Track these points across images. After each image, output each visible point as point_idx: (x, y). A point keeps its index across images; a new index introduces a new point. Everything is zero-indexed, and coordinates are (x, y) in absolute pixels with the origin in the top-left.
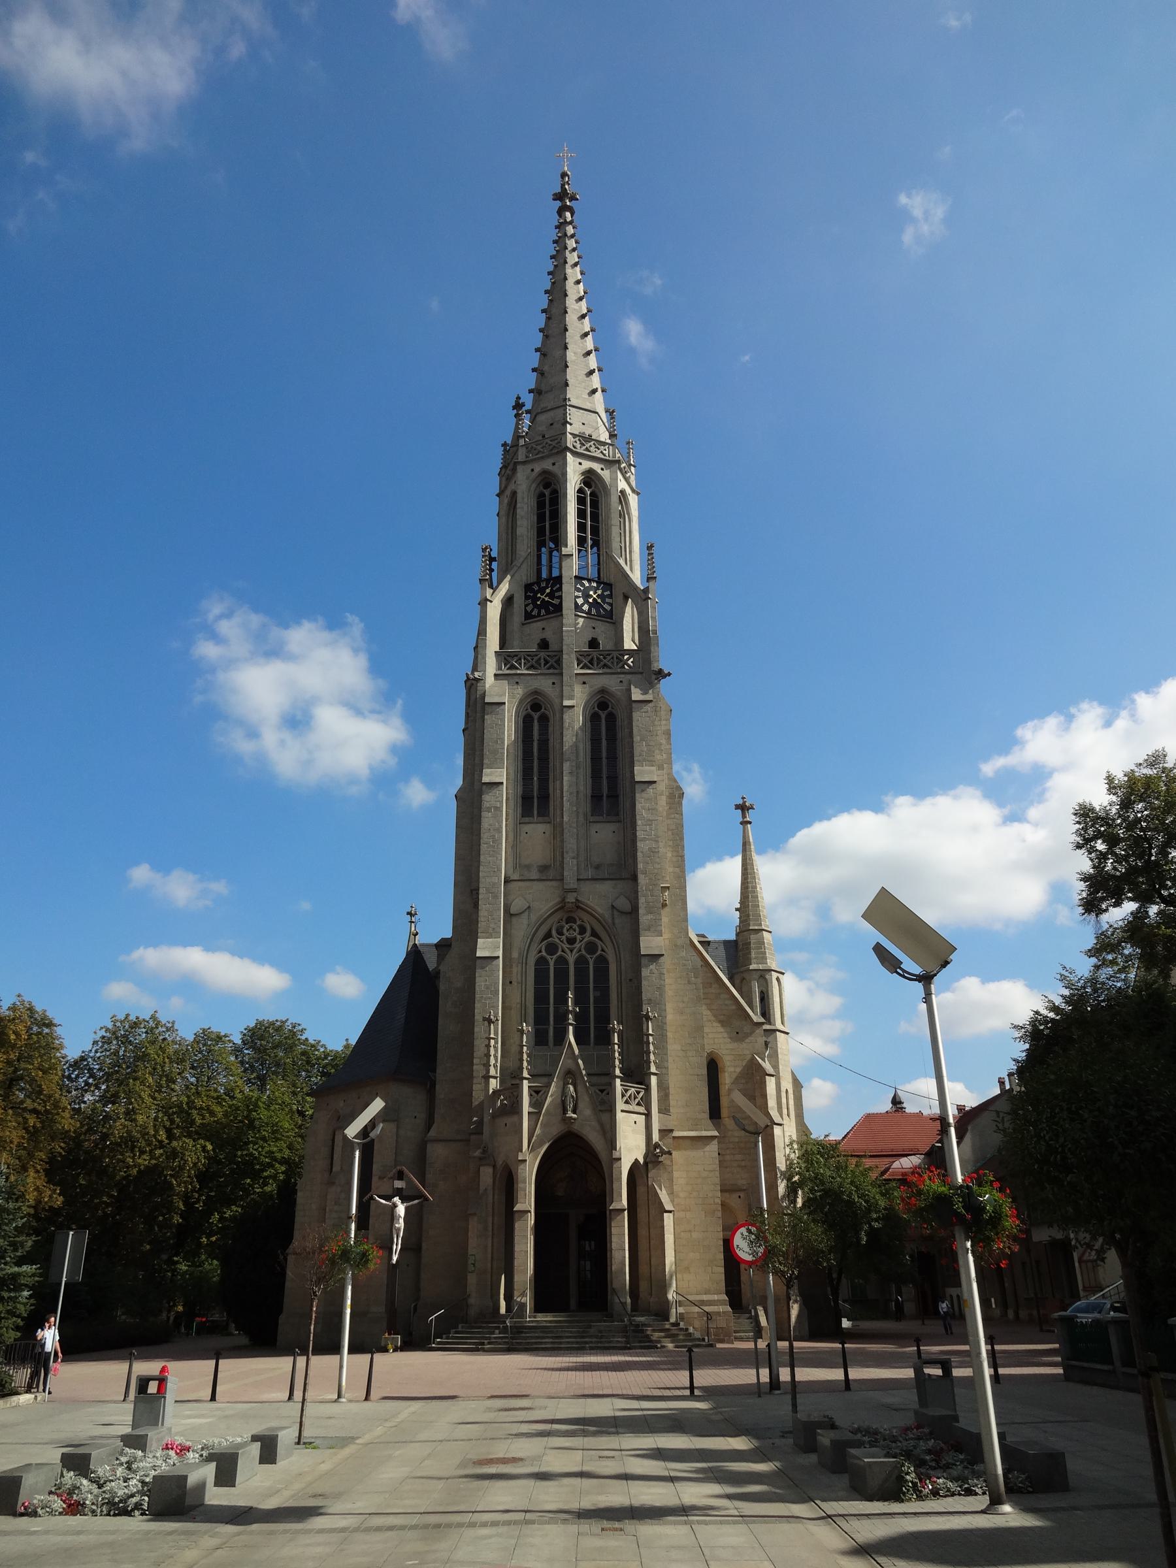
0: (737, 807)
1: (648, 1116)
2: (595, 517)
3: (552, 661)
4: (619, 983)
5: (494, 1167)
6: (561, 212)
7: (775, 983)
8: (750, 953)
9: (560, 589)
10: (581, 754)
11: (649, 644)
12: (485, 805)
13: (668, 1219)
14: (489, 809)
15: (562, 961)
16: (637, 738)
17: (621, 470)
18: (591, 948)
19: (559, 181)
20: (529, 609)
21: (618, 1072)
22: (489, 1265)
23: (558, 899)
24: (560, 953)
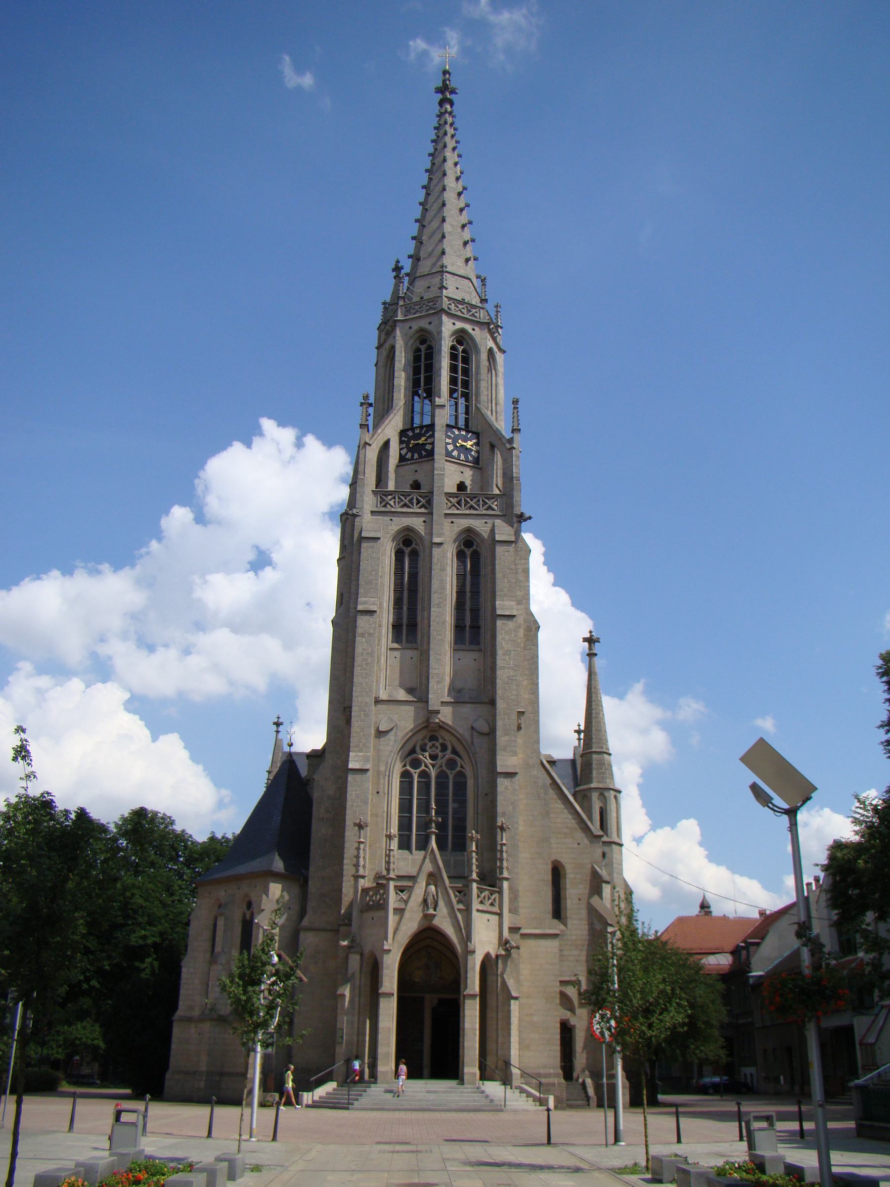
0: (585, 640)
1: (500, 915)
2: (466, 372)
3: (423, 501)
4: (477, 797)
5: (362, 954)
6: (441, 103)
7: (613, 800)
8: (591, 773)
9: (433, 436)
10: (448, 587)
11: (512, 489)
12: (359, 631)
13: (514, 1006)
14: (363, 635)
15: (424, 775)
16: (499, 575)
17: (490, 331)
18: (451, 764)
19: (441, 78)
20: (404, 452)
21: (474, 876)
22: (355, 1038)
23: (423, 719)
24: (423, 767)
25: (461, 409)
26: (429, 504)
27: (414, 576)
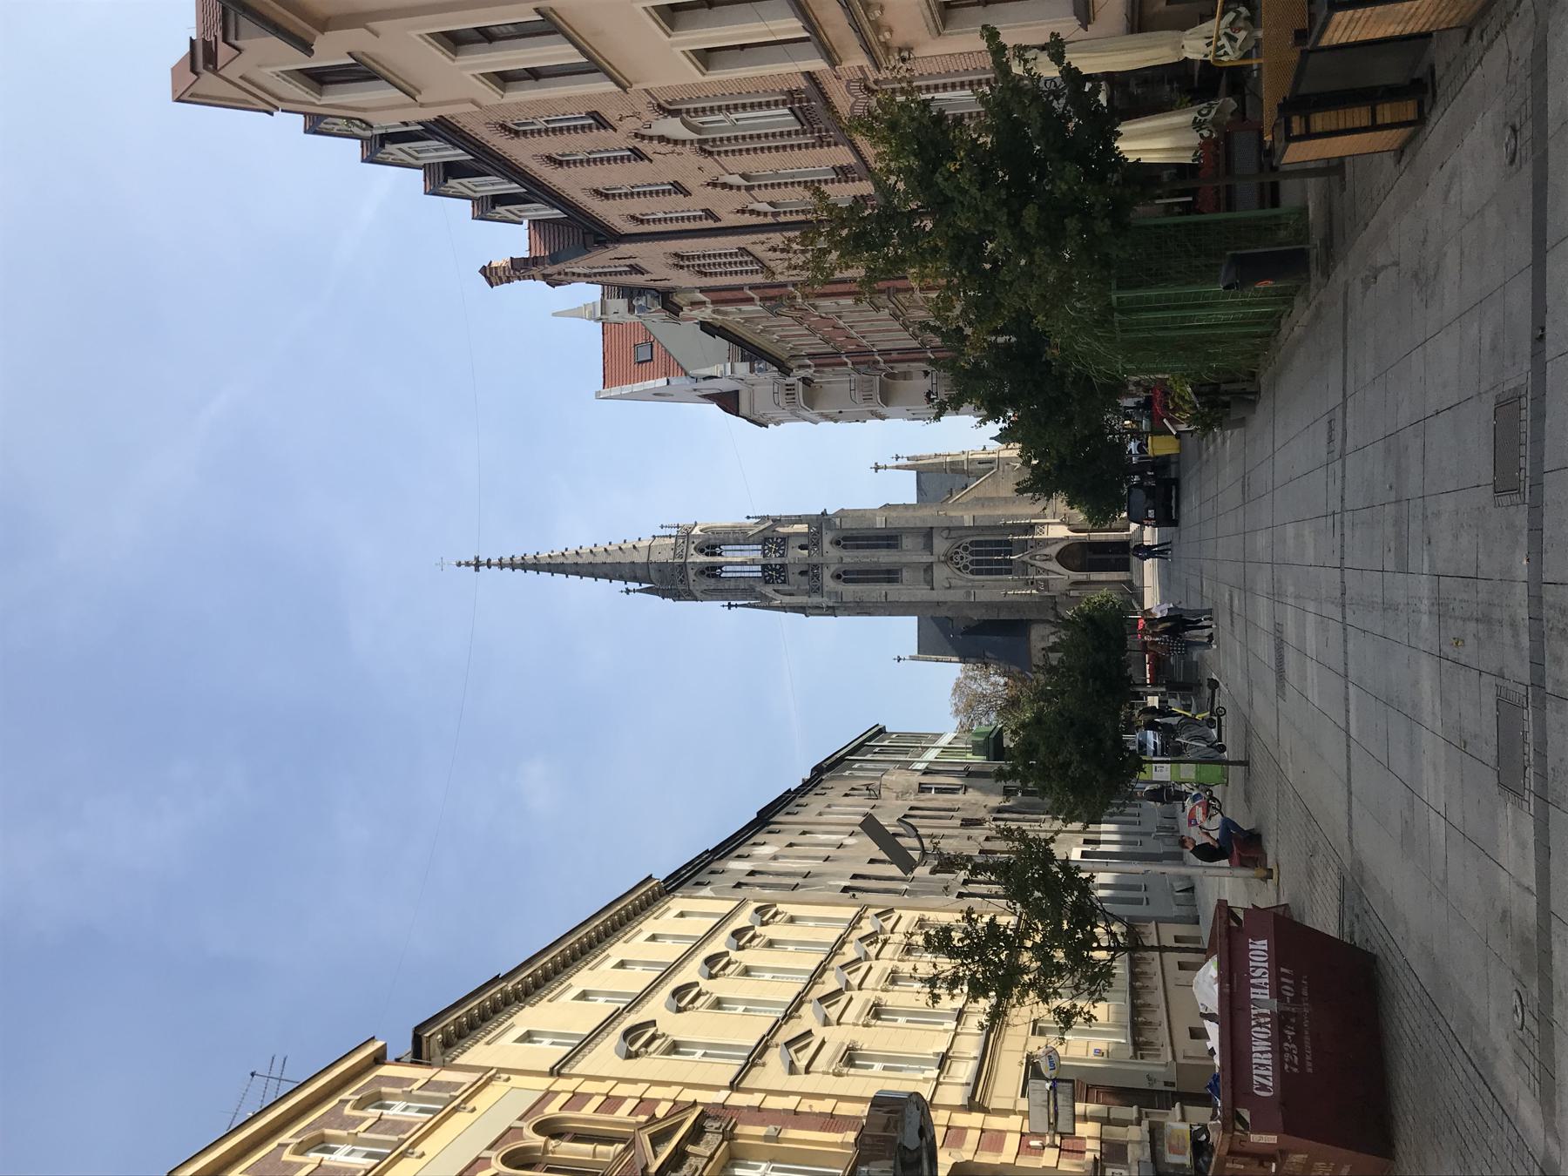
15: (971, 562)
18: (966, 549)
26: (815, 566)
27: (859, 572)
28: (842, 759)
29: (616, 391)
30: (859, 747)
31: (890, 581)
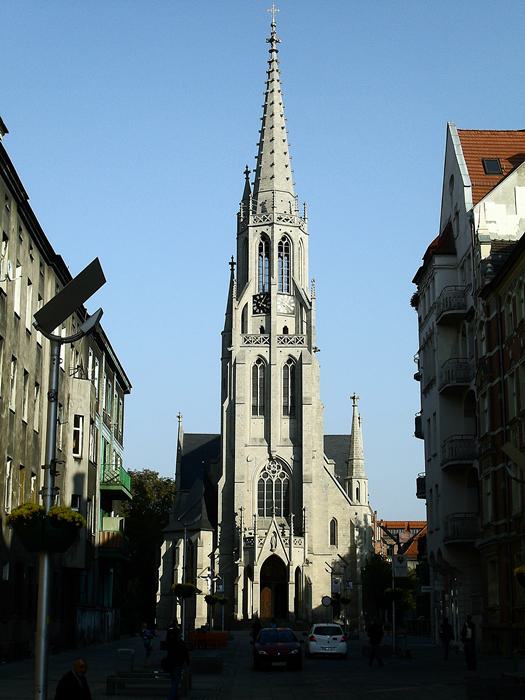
25: (285, 264)
28: (103, 348)
29: (456, 141)
30: (113, 369)
31: (254, 408)
